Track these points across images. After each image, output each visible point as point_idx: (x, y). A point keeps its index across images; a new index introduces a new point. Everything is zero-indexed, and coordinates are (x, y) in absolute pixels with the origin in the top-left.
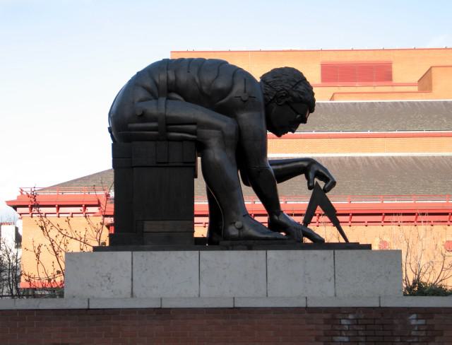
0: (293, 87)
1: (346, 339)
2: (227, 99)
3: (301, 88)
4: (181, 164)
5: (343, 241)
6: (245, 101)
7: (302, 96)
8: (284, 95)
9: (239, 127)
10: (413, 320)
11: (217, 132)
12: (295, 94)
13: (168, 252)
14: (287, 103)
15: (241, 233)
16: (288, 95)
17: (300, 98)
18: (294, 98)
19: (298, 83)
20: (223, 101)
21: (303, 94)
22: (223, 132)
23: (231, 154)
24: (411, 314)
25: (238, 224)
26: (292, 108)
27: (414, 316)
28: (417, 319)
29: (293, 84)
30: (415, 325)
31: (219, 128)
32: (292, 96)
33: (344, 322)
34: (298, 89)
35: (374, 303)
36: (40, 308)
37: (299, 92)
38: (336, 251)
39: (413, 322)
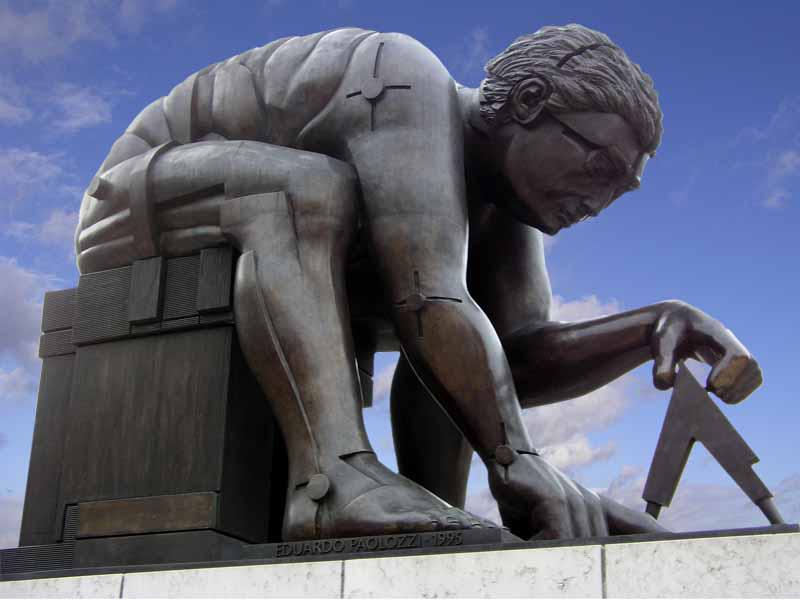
0: (562, 62)
2: (330, 106)
4: (195, 321)
5: (164, 318)
6: (374, 102)
7: (590, 87)
8: (533, 90)
9: (358, 180)
11: (267, 200)
12: (567, 82)
13: (29, 583)
14: (548, 116)
15: (325, 517)
16: (548, 89)
17: (588, 93)
18: (564, 93)
19: (581, 51)
20: (316, 120)
21: (595, 80)
22: (289, 197)
23: (321, 262)
25: (318, 484)
26: (569, 132)
29: (562, 54)
31: (277, 185)
34: (577, 69)
37: (585, 76)
38: (610, 548)
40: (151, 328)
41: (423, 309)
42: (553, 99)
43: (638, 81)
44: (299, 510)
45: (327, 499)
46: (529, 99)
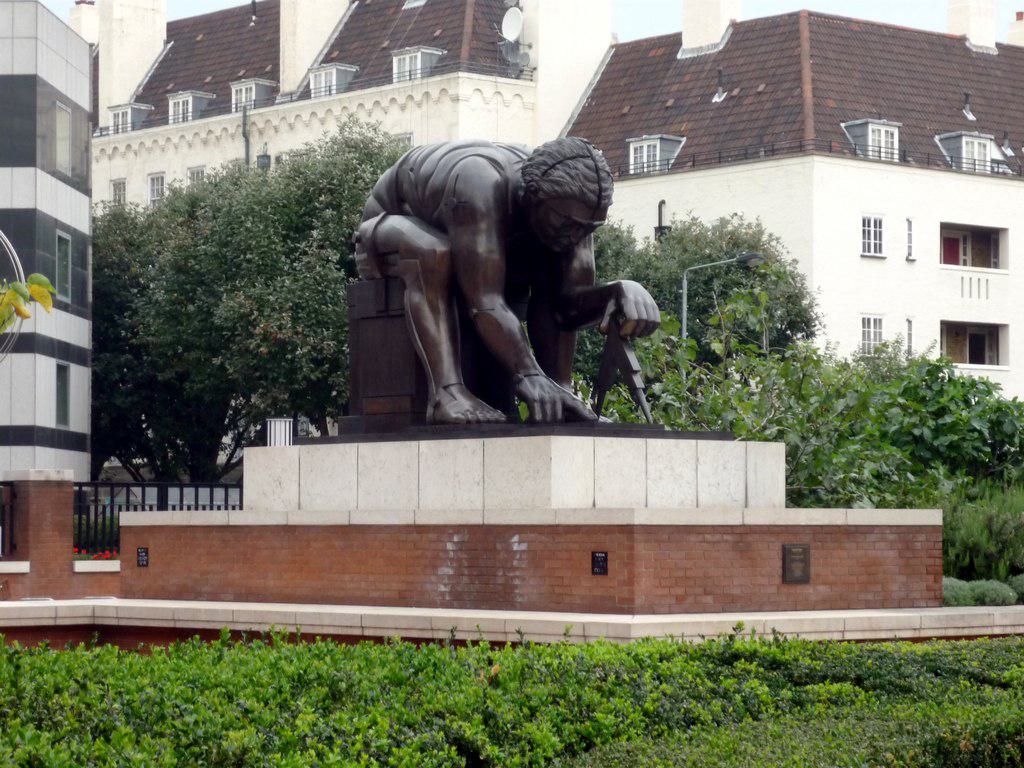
1: (451, 572)
3: (558, 173)
7: (556, 188)
8: (532, 189)
10: (517, 544)
12: (546, 186)
17: (556, 191)
24: (514, 535)
27: (516, 538)
28: (520, 542)
30: (517, 551)
32: (543, 190)
33: (450, 546)
35: (476, 520)
36: (192, 524)
39: (516, 547)
40: (383, 314)
41: (476, 315)
42: (541, 195)
43: (586, 177)
44: (430, 411)
45: (437, 405)
46: (531, 192)
